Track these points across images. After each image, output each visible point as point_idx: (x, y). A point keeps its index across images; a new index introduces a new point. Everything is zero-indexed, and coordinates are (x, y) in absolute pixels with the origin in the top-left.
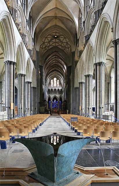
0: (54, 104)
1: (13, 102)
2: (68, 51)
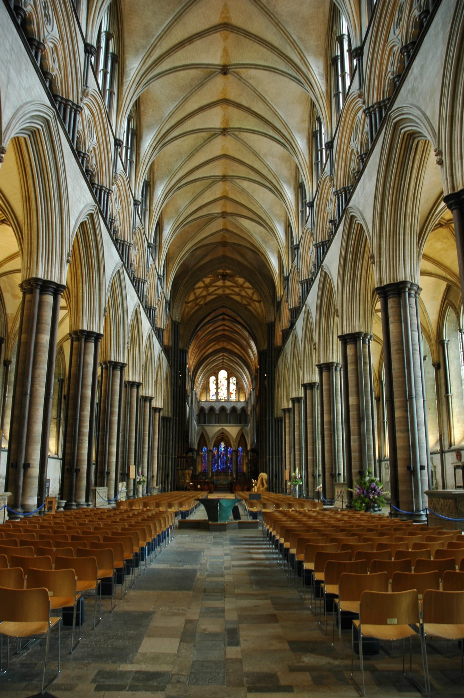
0: (219, 456)
1: (135, 464)
2: (259, 309)
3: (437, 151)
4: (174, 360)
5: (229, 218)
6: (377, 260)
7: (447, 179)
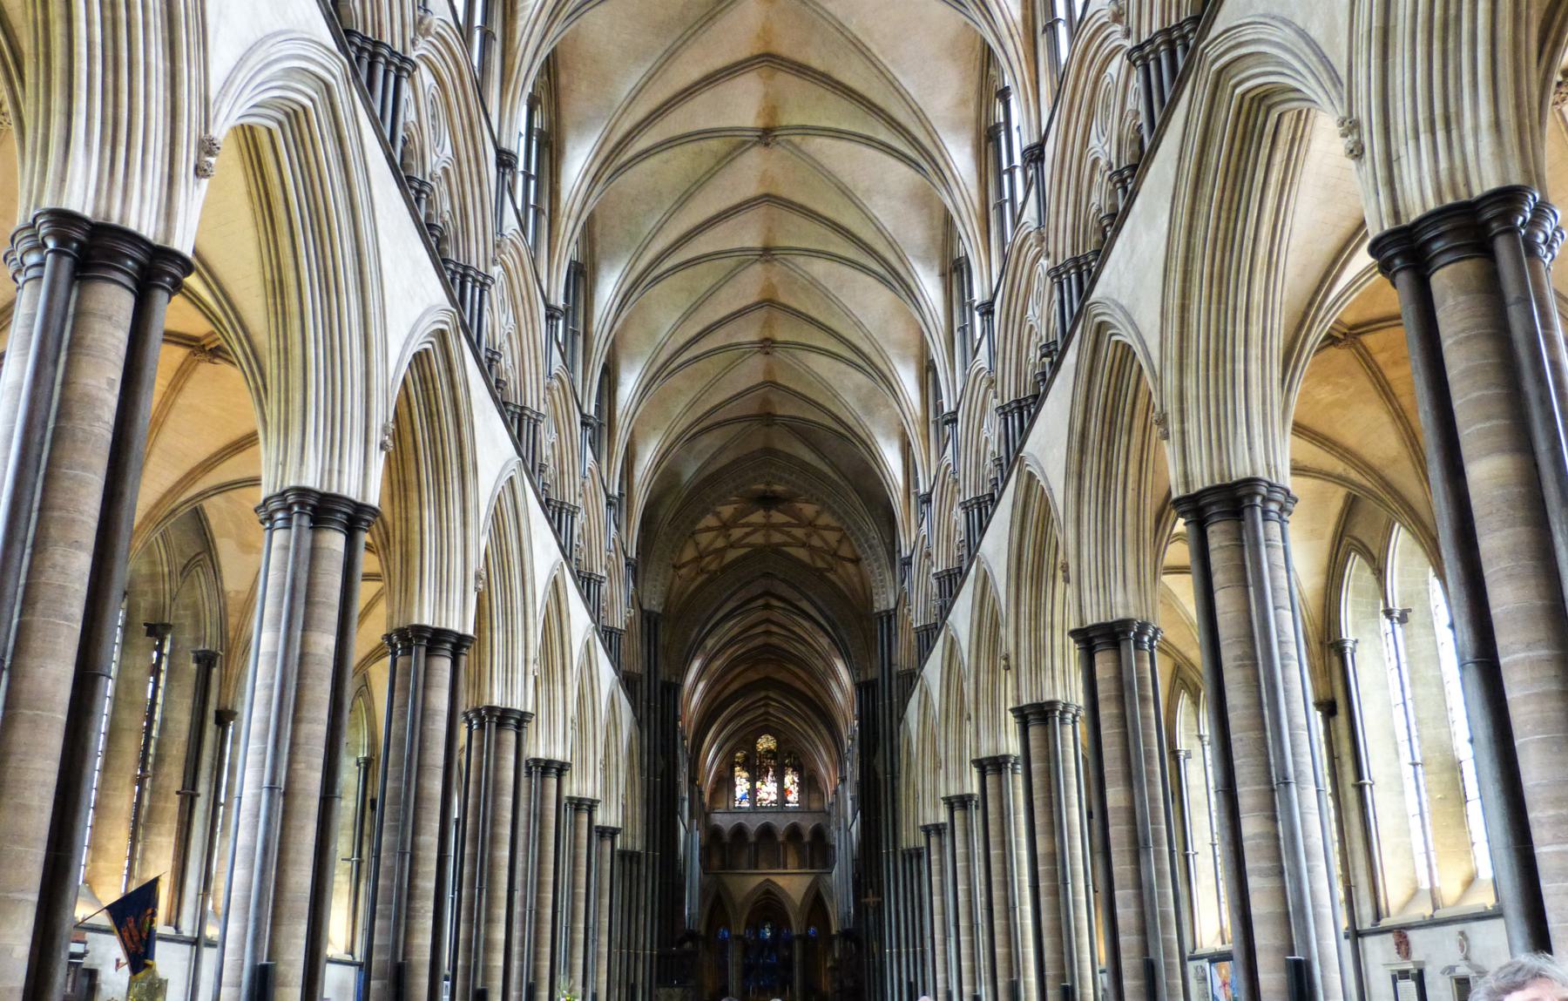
2: (856, 579)
3: (1347, 124)
4: (649, 707)
5: (779, 354)
6: (1174, 427)
7: (1378, 194)
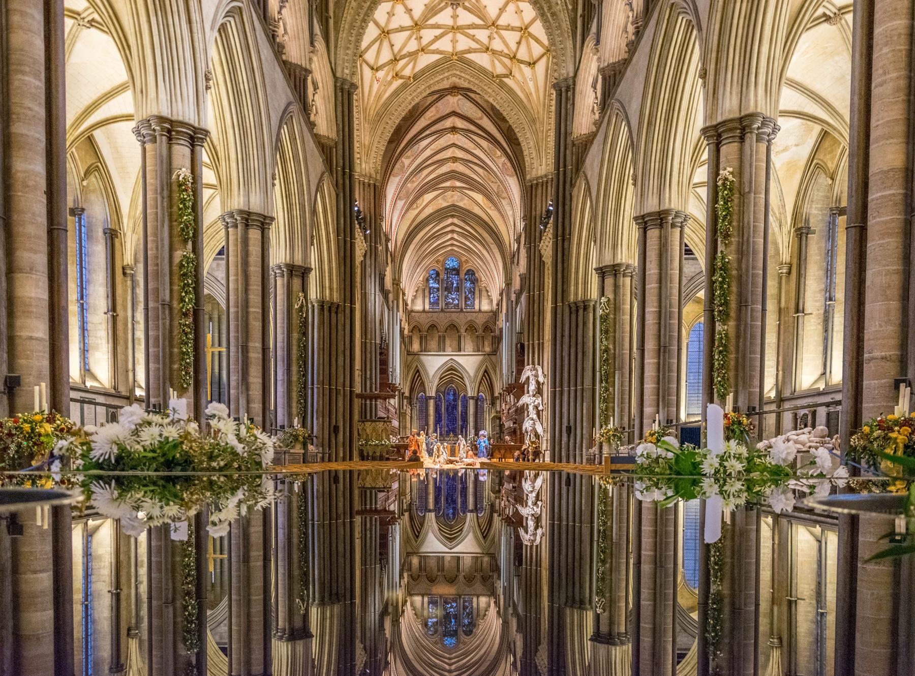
2: (531, 84)
4: (344, 173)
